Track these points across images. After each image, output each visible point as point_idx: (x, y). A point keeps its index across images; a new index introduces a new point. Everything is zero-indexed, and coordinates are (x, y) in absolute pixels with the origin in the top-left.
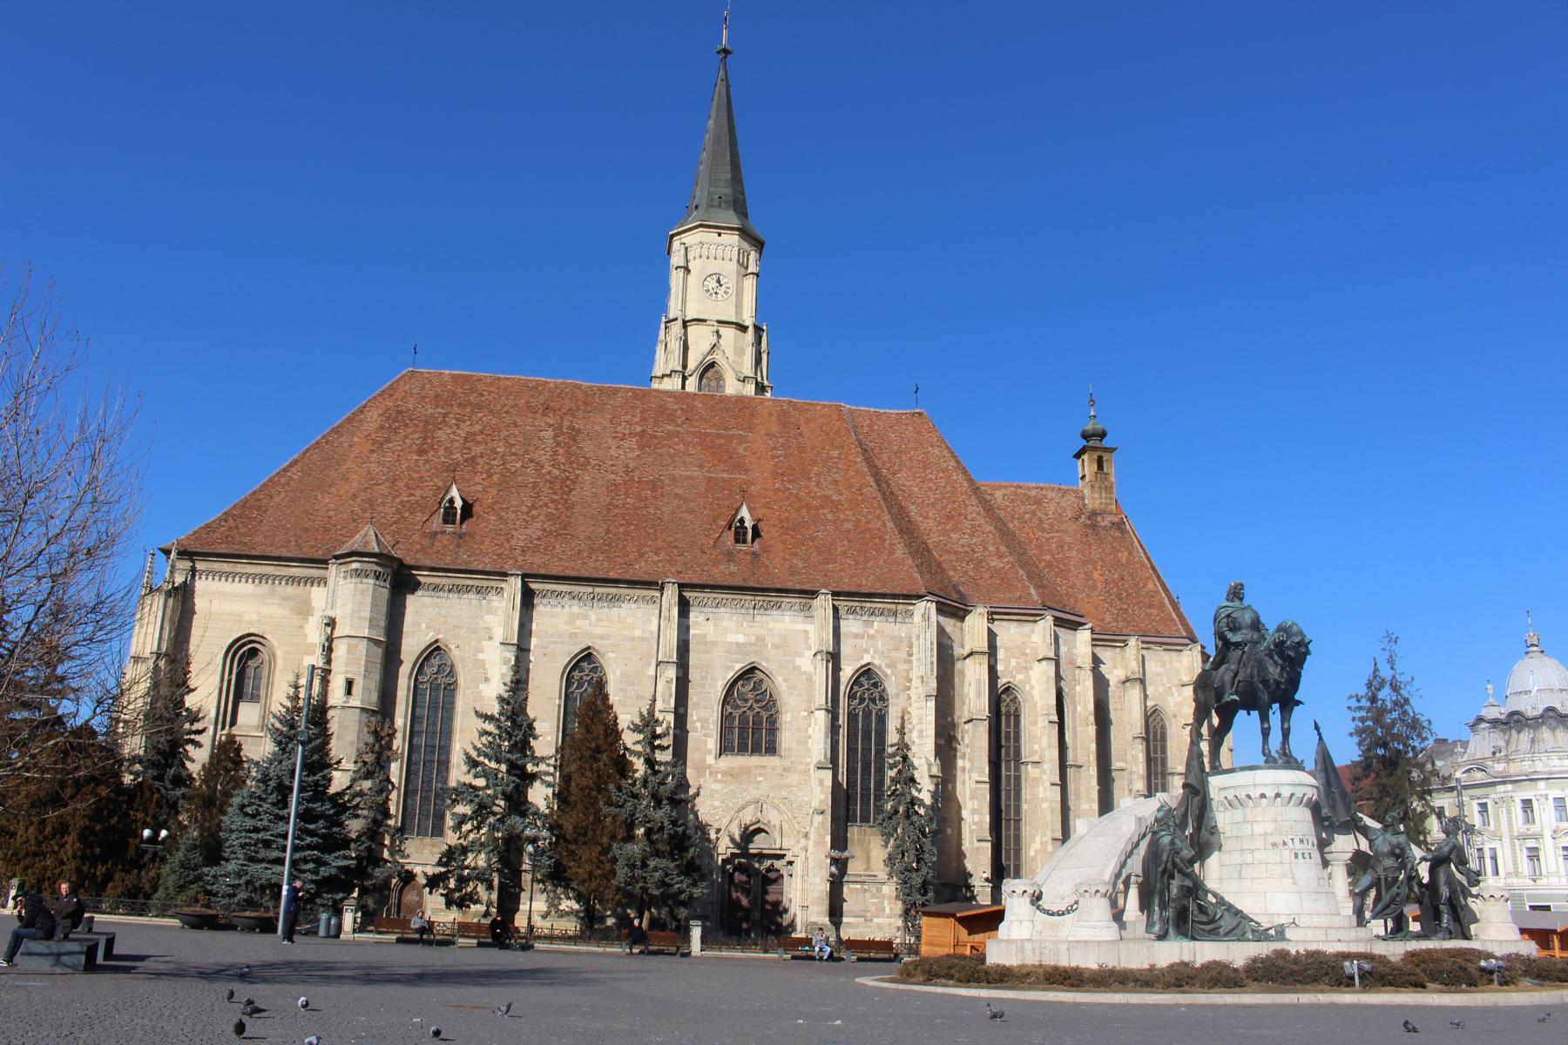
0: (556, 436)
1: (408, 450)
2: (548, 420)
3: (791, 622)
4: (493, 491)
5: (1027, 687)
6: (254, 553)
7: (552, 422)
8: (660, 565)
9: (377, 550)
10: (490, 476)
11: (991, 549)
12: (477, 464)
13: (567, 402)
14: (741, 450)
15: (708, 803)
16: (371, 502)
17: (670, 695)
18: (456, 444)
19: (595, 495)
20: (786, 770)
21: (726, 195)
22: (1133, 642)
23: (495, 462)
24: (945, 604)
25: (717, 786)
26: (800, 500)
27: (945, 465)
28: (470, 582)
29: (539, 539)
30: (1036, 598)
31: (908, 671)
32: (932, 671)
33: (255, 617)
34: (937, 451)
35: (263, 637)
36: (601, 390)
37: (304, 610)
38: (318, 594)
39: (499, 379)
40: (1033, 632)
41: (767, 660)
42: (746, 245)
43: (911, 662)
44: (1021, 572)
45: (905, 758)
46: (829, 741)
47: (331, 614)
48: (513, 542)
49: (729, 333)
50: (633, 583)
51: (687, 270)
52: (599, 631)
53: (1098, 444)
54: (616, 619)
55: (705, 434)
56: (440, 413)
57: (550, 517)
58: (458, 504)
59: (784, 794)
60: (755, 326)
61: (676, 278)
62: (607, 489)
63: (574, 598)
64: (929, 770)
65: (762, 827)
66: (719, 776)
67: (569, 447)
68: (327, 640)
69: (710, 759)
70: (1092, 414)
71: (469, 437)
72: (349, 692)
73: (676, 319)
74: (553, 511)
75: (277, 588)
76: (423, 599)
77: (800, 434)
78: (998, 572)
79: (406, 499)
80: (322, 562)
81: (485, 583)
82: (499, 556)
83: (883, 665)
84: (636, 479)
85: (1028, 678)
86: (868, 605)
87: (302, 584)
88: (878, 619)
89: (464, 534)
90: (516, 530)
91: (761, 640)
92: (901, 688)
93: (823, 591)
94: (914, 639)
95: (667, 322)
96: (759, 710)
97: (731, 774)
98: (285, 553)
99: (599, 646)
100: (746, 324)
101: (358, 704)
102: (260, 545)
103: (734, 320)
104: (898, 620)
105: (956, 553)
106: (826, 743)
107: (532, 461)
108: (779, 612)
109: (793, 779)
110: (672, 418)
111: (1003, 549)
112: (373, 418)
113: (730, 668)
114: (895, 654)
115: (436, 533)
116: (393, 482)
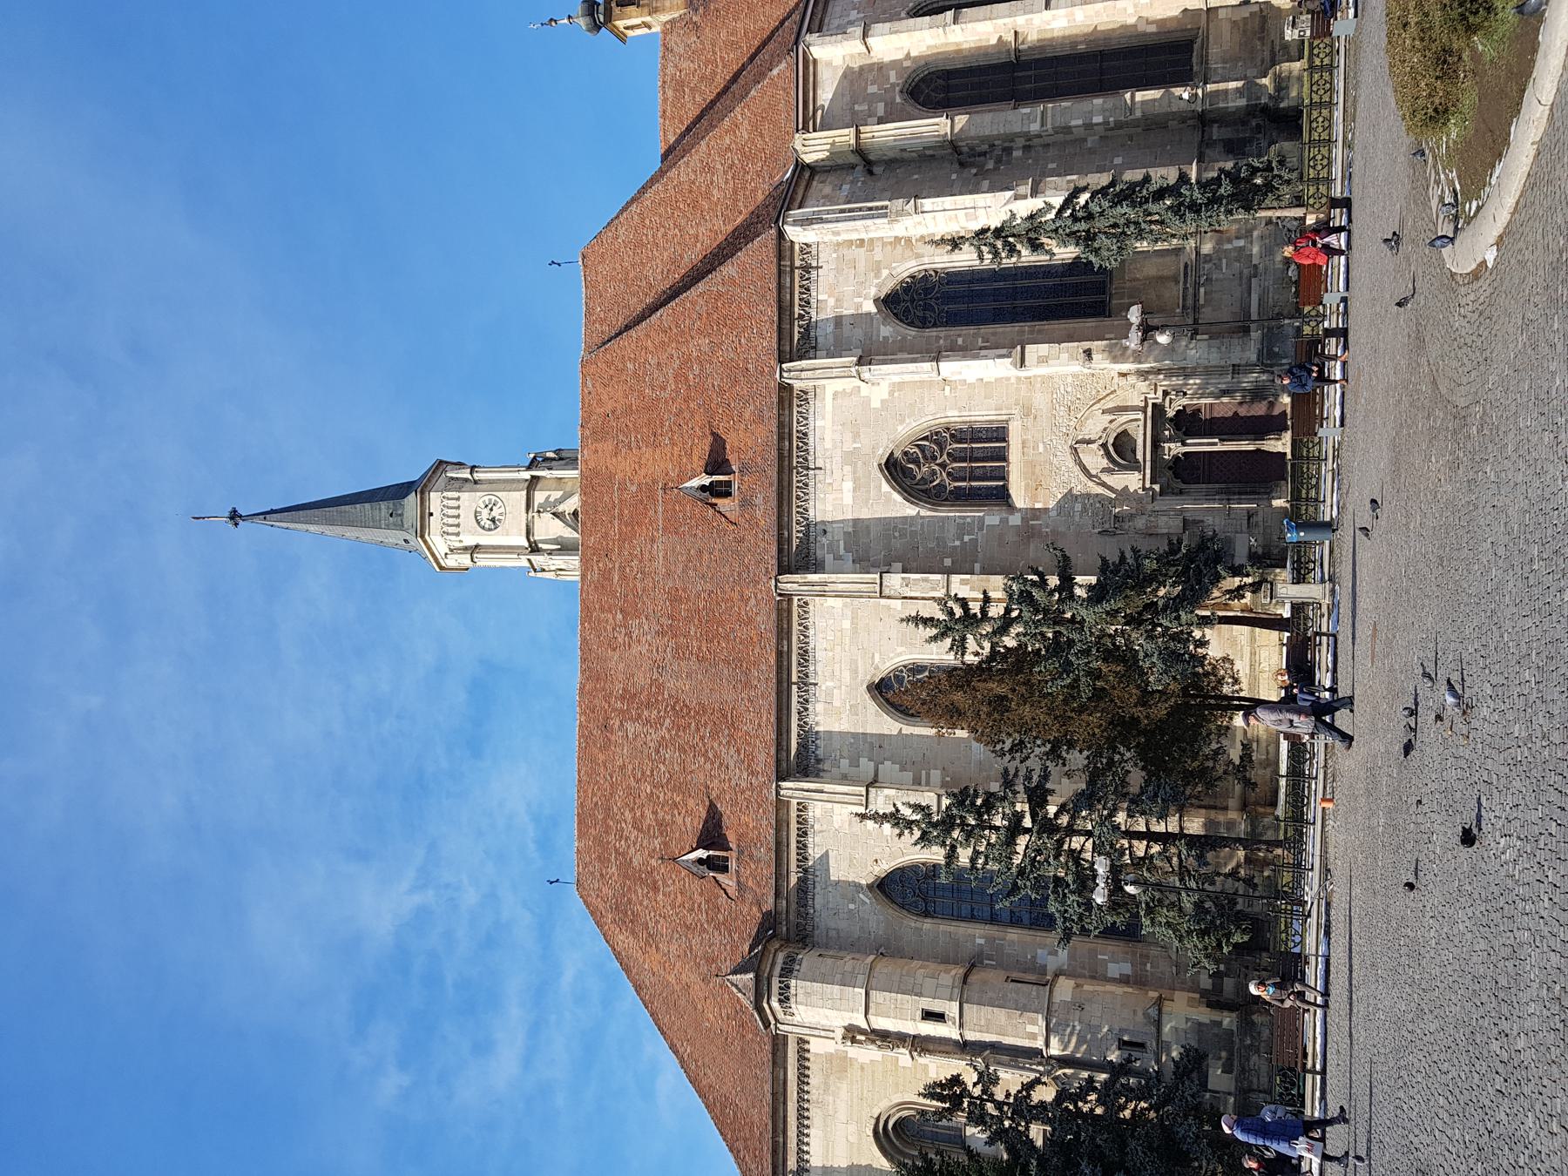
0: (631, 719)
1: (654, 903)
2: (616, 727)
3: (823, 418)
4: (691, 803)
5: (906, 64)
7: (618, 723)
8: (759, 596)
9: (751, 975)
10: (675, 805)
12: (664, 819)
13: (596, 701)
14: (634, 488)
15: (1077, 519)
17: (926, 580)
18: (644, 845)
19: (689, 675)
20: (1027, 411)
21: (388, 508)
23: (662, 795)
26: (681, 411)
28: (793, 845)
29: (738, 751)
30: (783, 65)
31: (884, 245)
33: (852, 1128)
34: (621, 231)
35: (878, 1119)
36: (584, 660)
37: (840, 1064)
38: (816, 1046)
39: (579, 781)
40: (829, 64)
42: (441, 482)
43: (871, 240)
44: (753, 93)
45: (998, 232)
46: (983, 352)
47: (839, 1033)
48: (744, 784)
49: (539, 497)
50: (783, 632)
51: (474, 549)
52: (847, 676)
53: (601, 8)
54: (831, 654)
55: (620, 534)
56: (616, 859)
57: (714, 735)
58: (702, 853)
59: (1062, 411)
60: (529, 468)
61: (484, 561)
62: (682, 660)
63: (806, 709)
64: (1025, 197)
65: (1111, 441)
67: (642, 703)
68: (873, 1042)
70: (566, 21)
71: (637, 826)
72: (939, 1017)
73: (529, 560)
74: (708, 731)
76: (817, 906)
77: (613, 412)
78: (755, 127)
79: (704, 915)
80: (779, 1043)
81: (794, 826)
82: (760, 806)
83: (876, 281)
84: (670, 622)
86: (797, 310)
87: (807, 1064)
89: (738, 846)
90: (730, 779)
91: (850, 458)
92: (908, 253)
93: (778, 376)
94: (840, 239)
95: (535, 570)
96: (945, 456)
98: (768, 1087)
100: (529, 477)
101: (955, 1006)
102: (760, 1115)
103: (525, 492)
104: (814, 264)
105: (735, 192)
106: (986, 357)
109: (1040, 400)
110: (606, 575)
112: (623, 939)
113: (888, 499)
114: (861, 266)
115: (738, 882)
116: (688, 928)
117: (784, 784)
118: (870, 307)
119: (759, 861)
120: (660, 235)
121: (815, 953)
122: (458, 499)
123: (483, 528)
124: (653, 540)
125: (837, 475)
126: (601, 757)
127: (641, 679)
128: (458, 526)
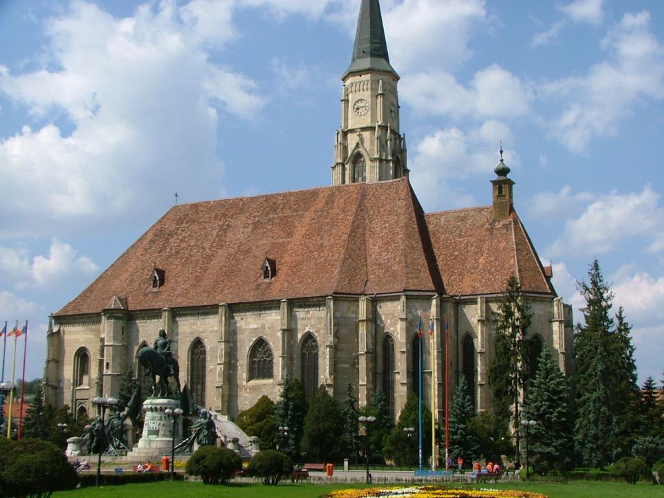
6: (80, 313)
7: (221, 223)
11: (398, 259)
16: (131, 281)
22: (479, 300)
24: (347, 297)
25: (247, 395)
27: (399, 211)
32: (331, 334)
33: (83, 340)
41: (266, 335)
49: (366, 134)
51: (346, 101)
52: (201, 330)
57: (197, 276)
66: (248, 390)
69: (244, 383)
70: (500, 158)
72: (107, 368)
74: (198, 274)
75: (90, 327)
77: (331, 208)
85: (396, 329)
88: (314, 309)
91: (263, 327)
97: (254, 389)
98: (90, 311)
99: (202, 336)
103: (369, 125)
105: (380, 264)
107: (202, 248)
108: (270, 312)
110: (275, 211)
111: (403, 258)
112: (150, 236)
114: (319, 326)
117: (167, 313)
118: (307, 330)
119: (151, 302)
120: (387, 225)
121: (124, 325)
122: (367, 89)
123: (355, 105)
124: (272, 238)
125: (258, 322)
126: (213, 215)
127: (230, 235)
128: (355, 91)
